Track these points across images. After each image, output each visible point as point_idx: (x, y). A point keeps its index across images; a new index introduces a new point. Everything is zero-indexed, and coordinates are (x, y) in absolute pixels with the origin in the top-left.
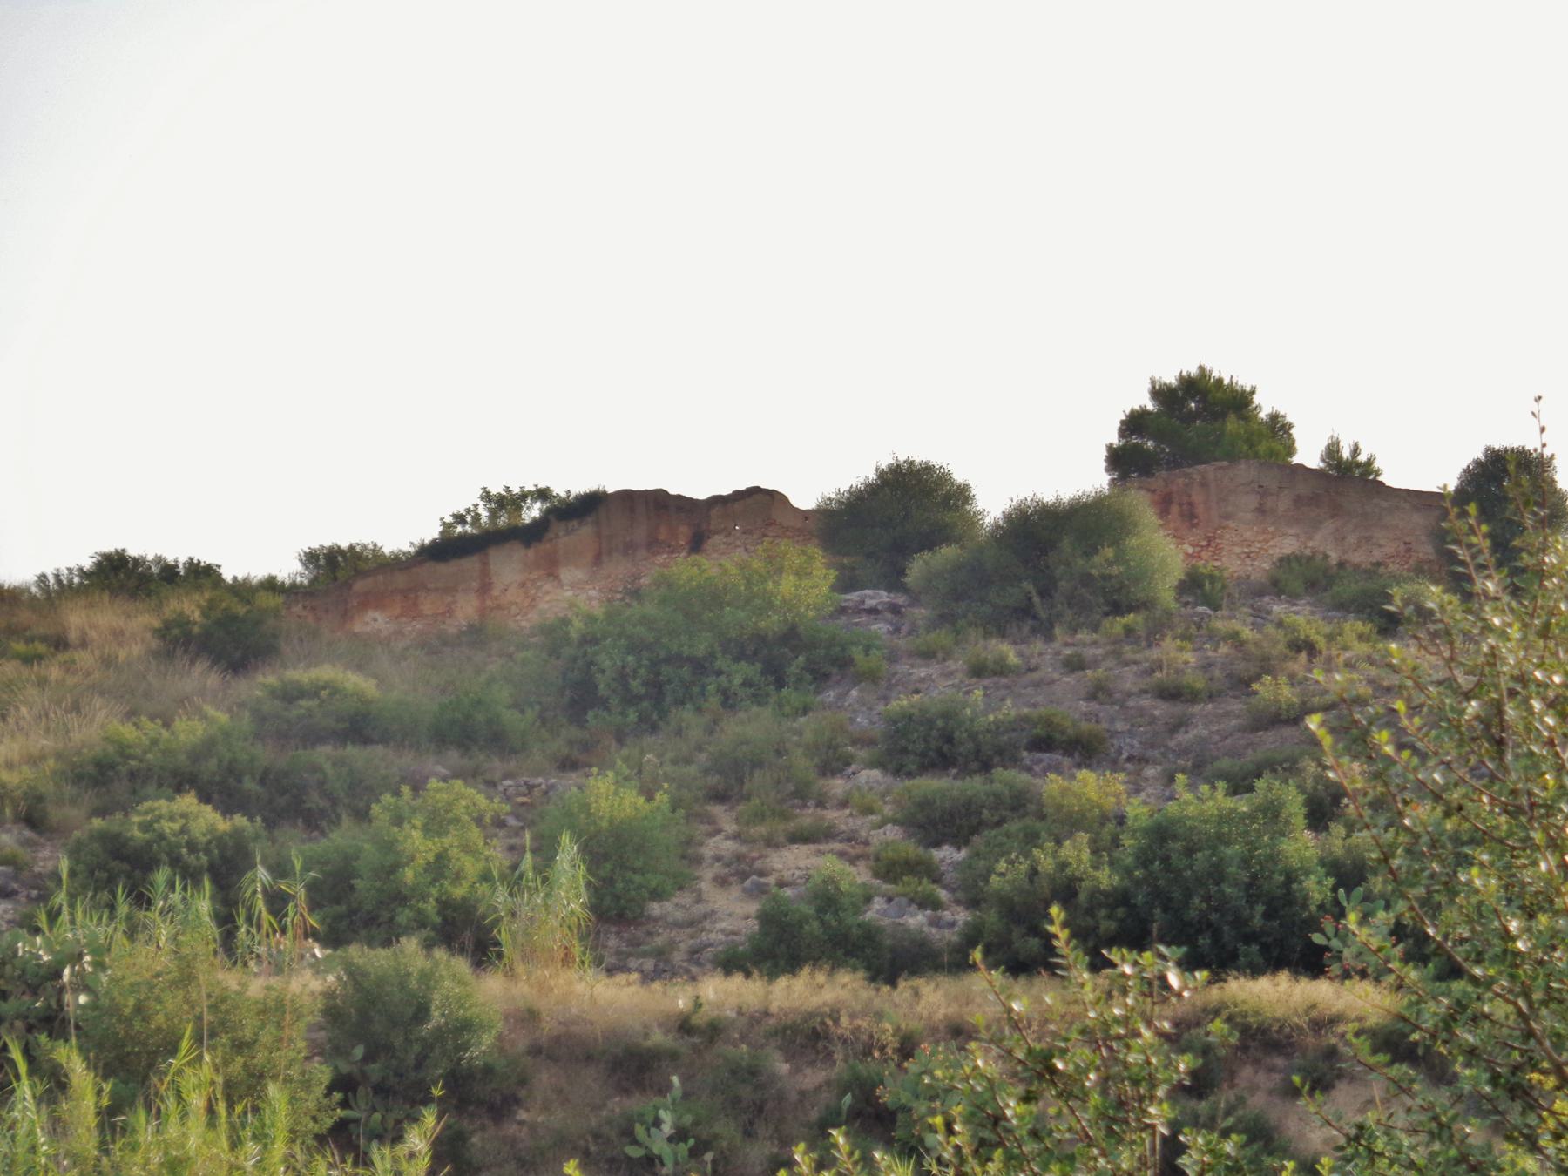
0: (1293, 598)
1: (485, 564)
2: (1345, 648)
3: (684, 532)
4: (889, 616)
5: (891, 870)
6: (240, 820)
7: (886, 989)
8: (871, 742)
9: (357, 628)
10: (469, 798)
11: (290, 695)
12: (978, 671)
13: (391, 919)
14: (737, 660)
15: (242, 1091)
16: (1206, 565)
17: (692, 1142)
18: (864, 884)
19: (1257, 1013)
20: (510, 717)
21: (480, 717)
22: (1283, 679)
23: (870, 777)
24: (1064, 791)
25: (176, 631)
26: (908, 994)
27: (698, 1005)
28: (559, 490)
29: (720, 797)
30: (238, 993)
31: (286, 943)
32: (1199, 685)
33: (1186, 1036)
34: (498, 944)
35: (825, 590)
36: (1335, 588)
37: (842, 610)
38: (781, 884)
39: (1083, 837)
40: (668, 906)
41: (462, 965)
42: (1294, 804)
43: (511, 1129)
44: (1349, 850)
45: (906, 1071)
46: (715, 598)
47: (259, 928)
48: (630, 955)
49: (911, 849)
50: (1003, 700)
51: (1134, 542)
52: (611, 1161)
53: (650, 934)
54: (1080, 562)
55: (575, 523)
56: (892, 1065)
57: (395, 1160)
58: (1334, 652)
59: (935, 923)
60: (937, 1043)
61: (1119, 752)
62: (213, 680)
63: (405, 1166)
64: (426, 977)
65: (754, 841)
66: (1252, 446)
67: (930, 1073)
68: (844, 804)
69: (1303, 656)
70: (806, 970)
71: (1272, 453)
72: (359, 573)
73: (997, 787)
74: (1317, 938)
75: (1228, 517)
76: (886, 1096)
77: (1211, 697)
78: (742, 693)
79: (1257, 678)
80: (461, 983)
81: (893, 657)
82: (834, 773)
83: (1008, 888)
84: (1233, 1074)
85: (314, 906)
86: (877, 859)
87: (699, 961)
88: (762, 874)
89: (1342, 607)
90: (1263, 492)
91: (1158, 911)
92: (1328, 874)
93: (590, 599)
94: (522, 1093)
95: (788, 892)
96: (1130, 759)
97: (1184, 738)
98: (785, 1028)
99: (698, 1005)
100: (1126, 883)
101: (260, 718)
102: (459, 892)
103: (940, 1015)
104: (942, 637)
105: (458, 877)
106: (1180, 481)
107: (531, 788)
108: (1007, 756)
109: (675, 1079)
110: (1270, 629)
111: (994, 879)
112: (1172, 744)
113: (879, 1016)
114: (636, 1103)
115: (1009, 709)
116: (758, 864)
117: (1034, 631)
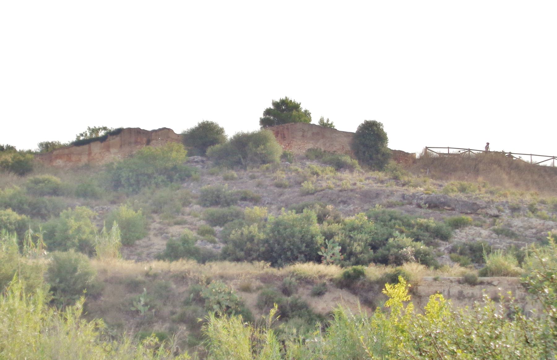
0: (312, 160)
1: (90, 147)
2: (327, 174)
3: (145, 139)
4: (201, 163)
5: (203, 233)
6: (24, 216)
7: (203, 265)
8: (197, 198)
9: (54, 164)
10: (87, 211)
11: (37, 182)
12: (226, 179)
13: (65, 244)
14: (160, 174)
15: (30, 289)
16: (289, 151)
17: (149, 306)
18: (195, 237)
19: (304, 273)
20: (97, 189)
21: (89, 189)
22: (310, 182)
23: (196, 207)
24: (250, 212)
25: (4, 164)
26: (209, 267)
27: (151, 268)
28: (109, 127)
29: (155, 212)
30: (26, 264)
31: (37, 250)
32: (287, 183)
33: (285, 279)
34: (95, 251)
35: (184, 156)
36: (324, 158)
37: (188, 162)
38: (172, 236)
39: (256, 225)
40: (141, 242)
41: (86, 257)
42: (314, 216)
43: (99, 302)
44: (328, 229)
45: (208, 288)
46: (154, 158)
47: (30, 246)
48: (131, 255)
49: (208, 227)
50: (233, 186)
51: (269, 144)
52: (127, 311)
53: (136, 249)
54: (254, 149)
55: (115, 136)
56: (204, 286)
57: (73, 310)
58: (324, 175)
59: (214, 247)
60: (216, 280)
61: (265, 201)
62: (15, 178)
63: (75, 312)
64: (76, 260)
65: (164, 224)
66: (300, 119)
67: (215, 288)
68: (189, 214)
69: (315, 176)
70: (180, 260)
71: (305, 121)
72: (55, 149)
73: (232, 210)
74: (320, 253)
75: (293, 138)
76: (202, 295)
77: (290, 187)
78: (161, 184)
79: (303, 182)
80: (86, 262)
81: (203, 175)
82: (187, 206)
83: (235, 238)
84: (297, 290)
85: (45, 240)
86: (198, 230)
87: (150, 257)
88: (167, 233)
89: (325, 163)
90: (304, 131)
91: (276, 245)
92: (323, 236)
93: (119, 157)
94: (102, 292)
95: (174, 238)
96: (267, 203)
97: (283, 198)
98: (175, 275)
99: (151, 268)
100: (268, 237)
101: (29, 189)
102: (84, 237)
103: (217, 272)
104: (216, 169)
105: (84, 233)
106: (281, 128)
107: (103, 209)
108: (234, 202)
109: (145, 289)
110: (306, 168)
111: (231, 236)
112: (279, 199)
113: (201, 272)
114: (134, 296)
115: (235, 189)
116: (166, 231)
117: (241, 168)
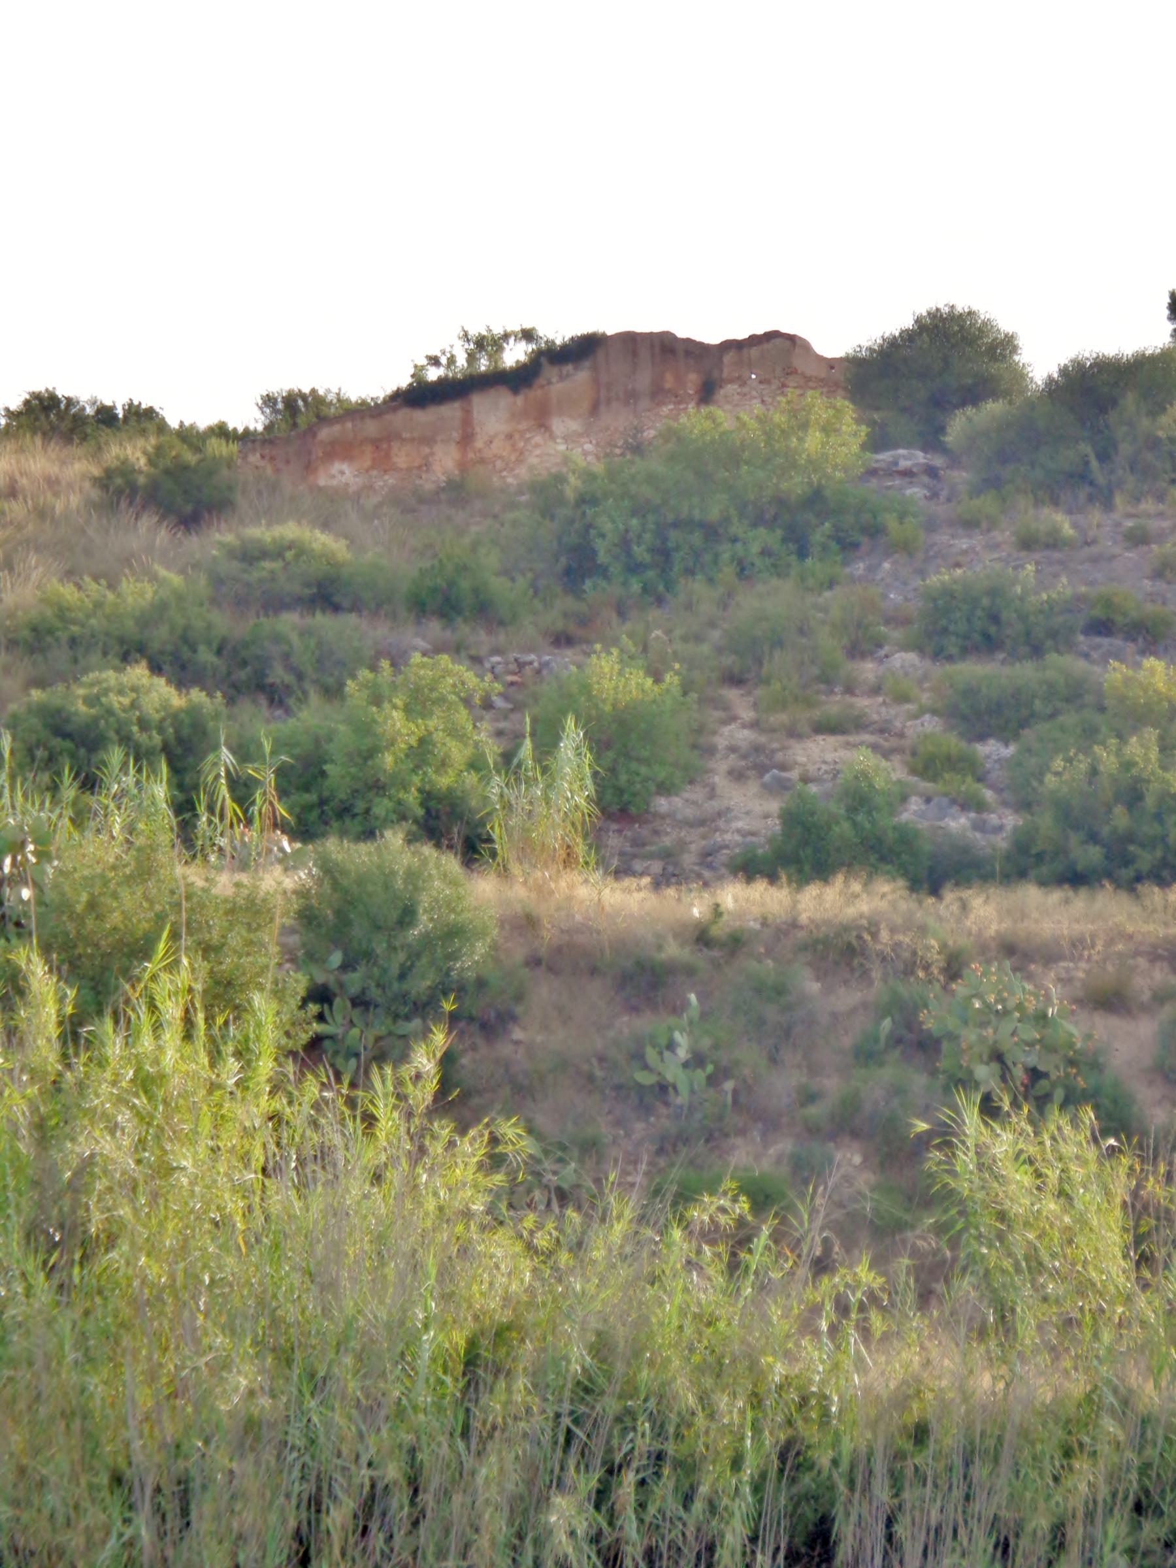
1: (468, 412)
3: (693, 379)
4: (925, 479)
5: (929, 766)
6: (197, 695)
7: (931, 900)
8: (906, 622)
11: (250, 555)
12: (1027, 543)
13: (367, 811)
14: (754, 525)
15: (224, 995)
17: (710, 1068)
18: (899, 781)
20: (498, 585)
21: (465, 584)
24: (1127, 681)
25: (119, 481)
26: (955, 908)
29: (735, 680)
30: (203, 890)
31: (252, 835)
34: (489, 840)
35: (855, 448)
37: (873, 472)
38: (806, 779)
39: (1151, 734)
40: (677, 801)
41: (452, 863)
43: (504, 1049)
45: (953, 993)
46: (732, 455)
48: (635, 856)
49: (953, 743)
50: (1056, 576)
52: (618, 1088)
53: (656, 832)
54: (1145, 422)
55: (569, 368)
56: (937, 986)
57: (399, 1083)
59: (979, 826)
60: (988, 962)
62: (163, 536)
64: (412, 876)
65: (773, 730)
68: (876, 690)
70: (839, 879)
72: (322, 419)
73: (1050, 674)
76: (929, 1022)
78: (758, 562)
81: (931, 526)
85: (283, 793)
86: (914, 754)
87: (715, 865)
88: (783, 767)
93: (585, 454)
94: (519, 1010)
95: (813, 789)
98: (817, 941)
99: (717, 911)
101: (217, 581)
102: (444, 781)
103: (993, 929)
104: (987, 503)
105: (443, 764)
107: (521, 665)
108: (1060, 638)
109: (693, 997)
111: (1049, 779)
113: (923, 930)
114: (646, 1023)
115: (1064, 587)
116: (779, 757)
117: (1091, 499)
